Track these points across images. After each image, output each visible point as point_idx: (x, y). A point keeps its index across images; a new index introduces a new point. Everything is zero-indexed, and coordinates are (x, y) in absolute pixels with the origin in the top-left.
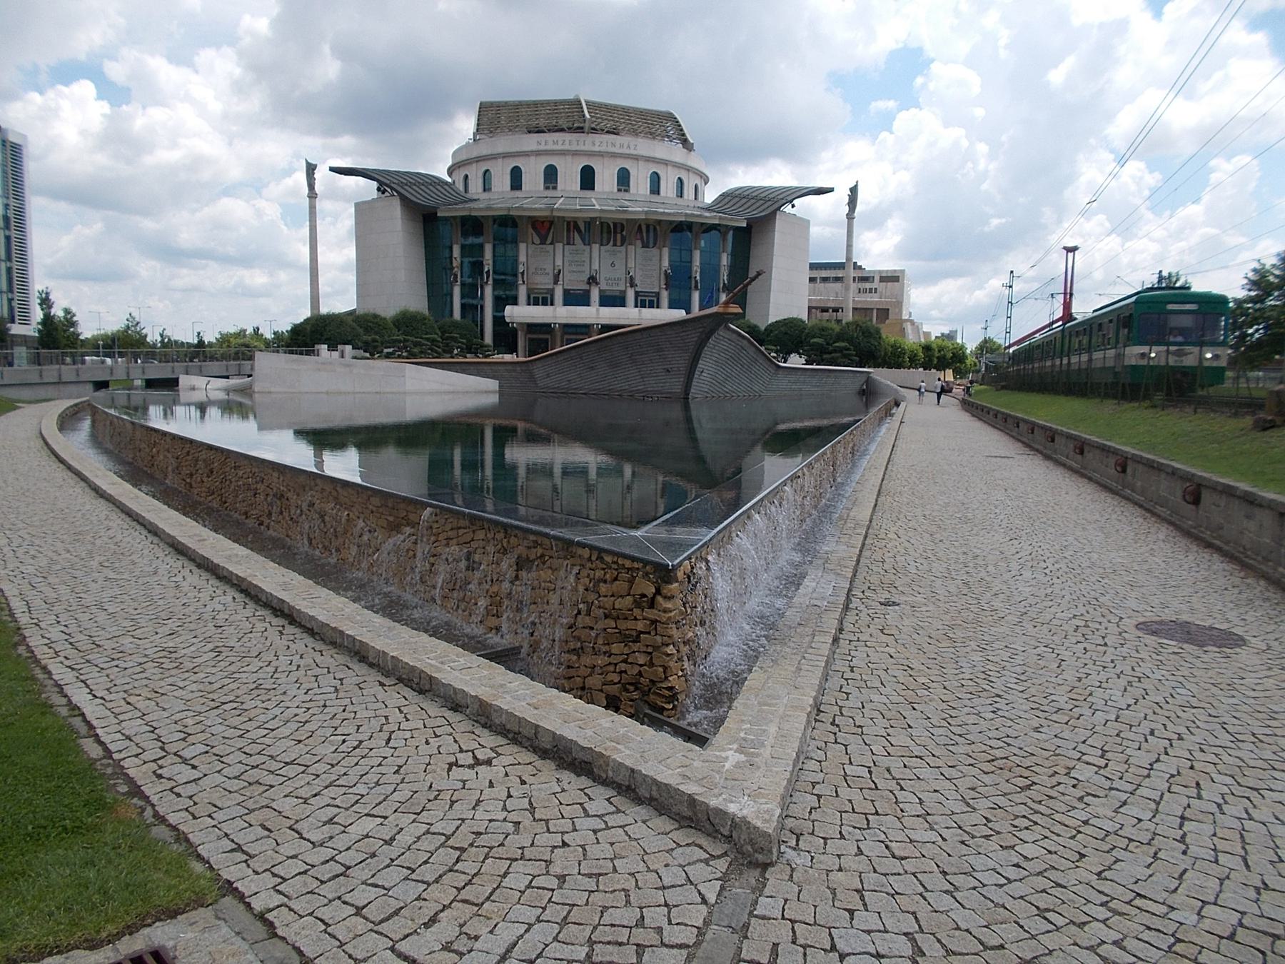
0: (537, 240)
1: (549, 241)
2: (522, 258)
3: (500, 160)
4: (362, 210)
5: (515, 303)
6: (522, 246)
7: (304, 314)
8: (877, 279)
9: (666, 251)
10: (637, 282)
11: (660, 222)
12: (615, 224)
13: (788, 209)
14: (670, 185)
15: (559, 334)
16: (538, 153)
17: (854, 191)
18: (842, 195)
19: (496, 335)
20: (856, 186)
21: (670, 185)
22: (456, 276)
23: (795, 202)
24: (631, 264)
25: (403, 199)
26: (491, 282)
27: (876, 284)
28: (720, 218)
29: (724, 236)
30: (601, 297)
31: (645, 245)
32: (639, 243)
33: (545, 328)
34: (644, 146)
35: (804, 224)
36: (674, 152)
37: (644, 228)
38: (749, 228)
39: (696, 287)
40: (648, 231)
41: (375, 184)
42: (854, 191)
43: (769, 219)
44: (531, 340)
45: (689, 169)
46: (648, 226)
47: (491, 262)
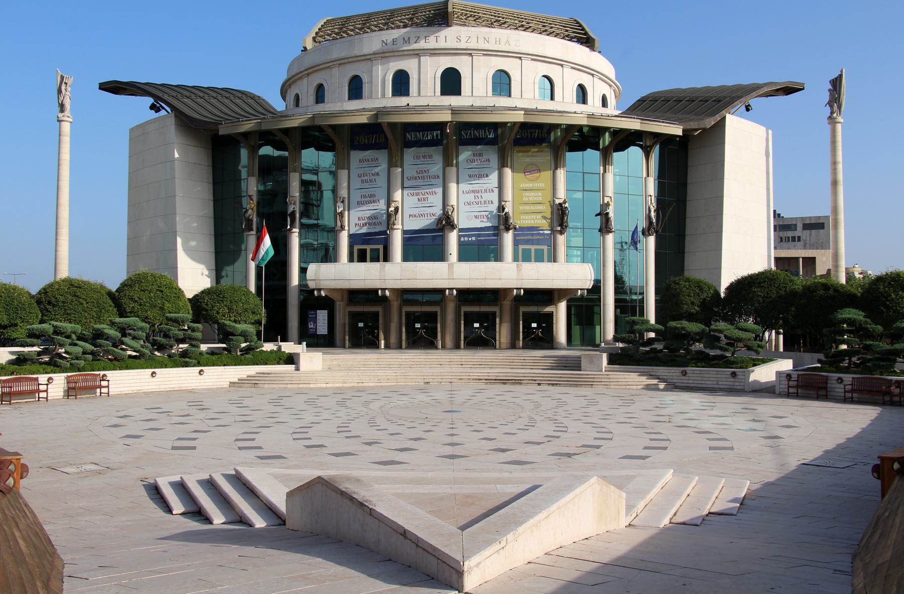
7: (52, 280)
8: (800, 227)
15: (395, 305)
17: (836, 83)
20: (841, 76)
27: (799, 232)
30: (461, 244)
33: (369, 296)
41: (150, 101)
42: (836, 83)
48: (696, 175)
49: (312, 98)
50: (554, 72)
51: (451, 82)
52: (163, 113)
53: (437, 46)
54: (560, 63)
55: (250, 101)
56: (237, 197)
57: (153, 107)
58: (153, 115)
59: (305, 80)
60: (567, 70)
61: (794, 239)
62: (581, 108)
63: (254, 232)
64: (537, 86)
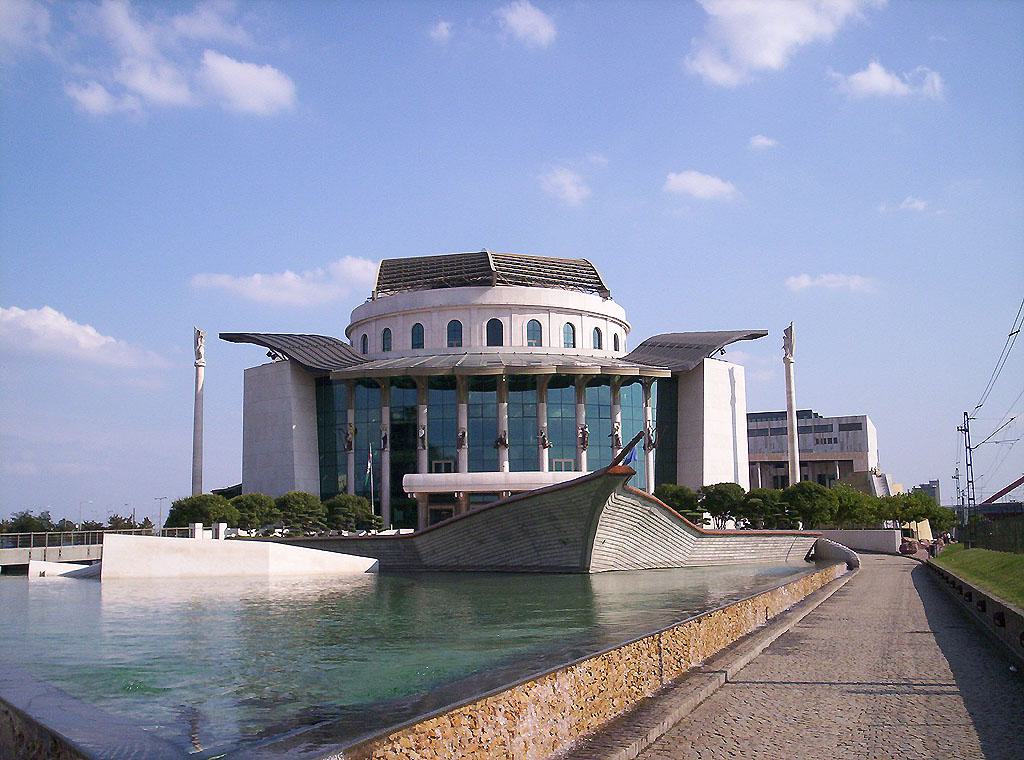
4: (253, 377)
5: (415, 471)
8: (836, 427)
15: (464, 504)
16: (440, 309)
17: (788, 332)
18: (776, 338)
19: (393, 507)
27: (835, 433)
33: (447, 498)
42: (788, 332)
44: (431, 510)
48: (683, 403)
49: (380, 341)
50: (575, 320)
51: (495, 333)
54: (580, 313)
57: (269, 354)
59: (373, 324)
62: (598, 353)
63: (353, 451)
64: (562, 332)
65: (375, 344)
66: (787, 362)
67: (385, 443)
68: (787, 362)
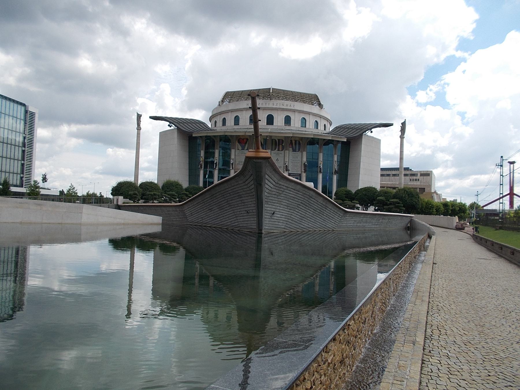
0: (240, 148)
1: (246, 148)
2: (233, 157)
3: (230, 113)
4: (163, 135)
6: (233, 151)
8: (419, 175)
9: (305, 153)
10: (290, 169)
11: (302, 138)
12: (279, 140)
13: (368, 133)
14: (311, 124)
17: (404, 125)
18: (396, 128)
21: (311, 124)
22: (201, 165)
23: (373, 130)
24: (287, 160)
25: (178, 129)
26: (217, 168)
27: (418, 177)
28: (332, 137)
29: (335, 146)
31: (294, 150)
32: (291, 149)
34: (299, 106)
35: (377, 142)
36: (315, 109)
37: (294, 142)
38: (348, 142)
39: (320, 172)
40: (295, 144)
41: (168, 123)
42: (404, 125)
43: (359, 138)
45: (321, 117)
46: (296, 141)
47: (218, 159)
49: (221, 123)
52: (172, 128)
53: (266, 106)
55: (202, 125)
56: (198, 157)
57: (169, 125)
58: (169, 128)
60: (311, 116)
61: (416, 180)
65: (220, 123)
66: (402, 137)
67: (216, 166)
68: (402, 137)
